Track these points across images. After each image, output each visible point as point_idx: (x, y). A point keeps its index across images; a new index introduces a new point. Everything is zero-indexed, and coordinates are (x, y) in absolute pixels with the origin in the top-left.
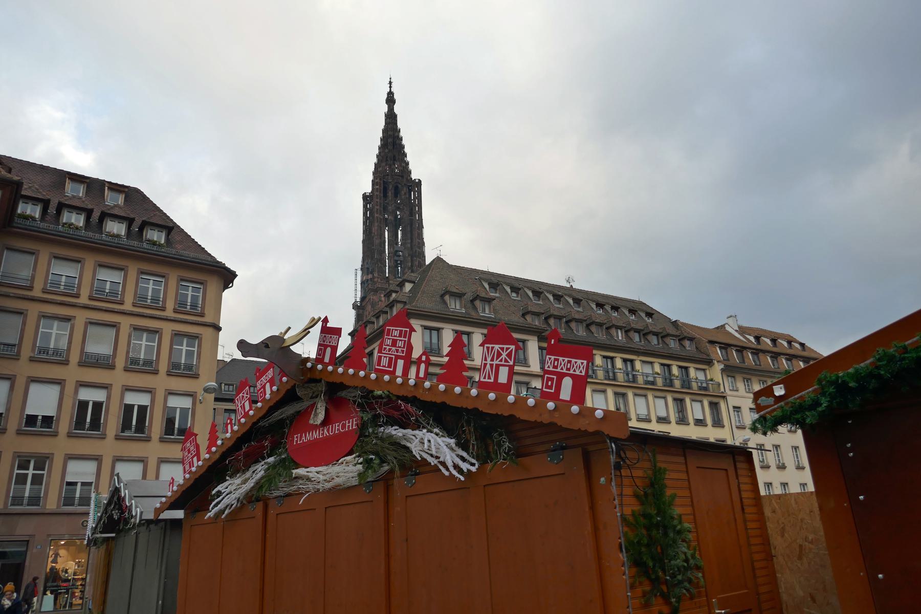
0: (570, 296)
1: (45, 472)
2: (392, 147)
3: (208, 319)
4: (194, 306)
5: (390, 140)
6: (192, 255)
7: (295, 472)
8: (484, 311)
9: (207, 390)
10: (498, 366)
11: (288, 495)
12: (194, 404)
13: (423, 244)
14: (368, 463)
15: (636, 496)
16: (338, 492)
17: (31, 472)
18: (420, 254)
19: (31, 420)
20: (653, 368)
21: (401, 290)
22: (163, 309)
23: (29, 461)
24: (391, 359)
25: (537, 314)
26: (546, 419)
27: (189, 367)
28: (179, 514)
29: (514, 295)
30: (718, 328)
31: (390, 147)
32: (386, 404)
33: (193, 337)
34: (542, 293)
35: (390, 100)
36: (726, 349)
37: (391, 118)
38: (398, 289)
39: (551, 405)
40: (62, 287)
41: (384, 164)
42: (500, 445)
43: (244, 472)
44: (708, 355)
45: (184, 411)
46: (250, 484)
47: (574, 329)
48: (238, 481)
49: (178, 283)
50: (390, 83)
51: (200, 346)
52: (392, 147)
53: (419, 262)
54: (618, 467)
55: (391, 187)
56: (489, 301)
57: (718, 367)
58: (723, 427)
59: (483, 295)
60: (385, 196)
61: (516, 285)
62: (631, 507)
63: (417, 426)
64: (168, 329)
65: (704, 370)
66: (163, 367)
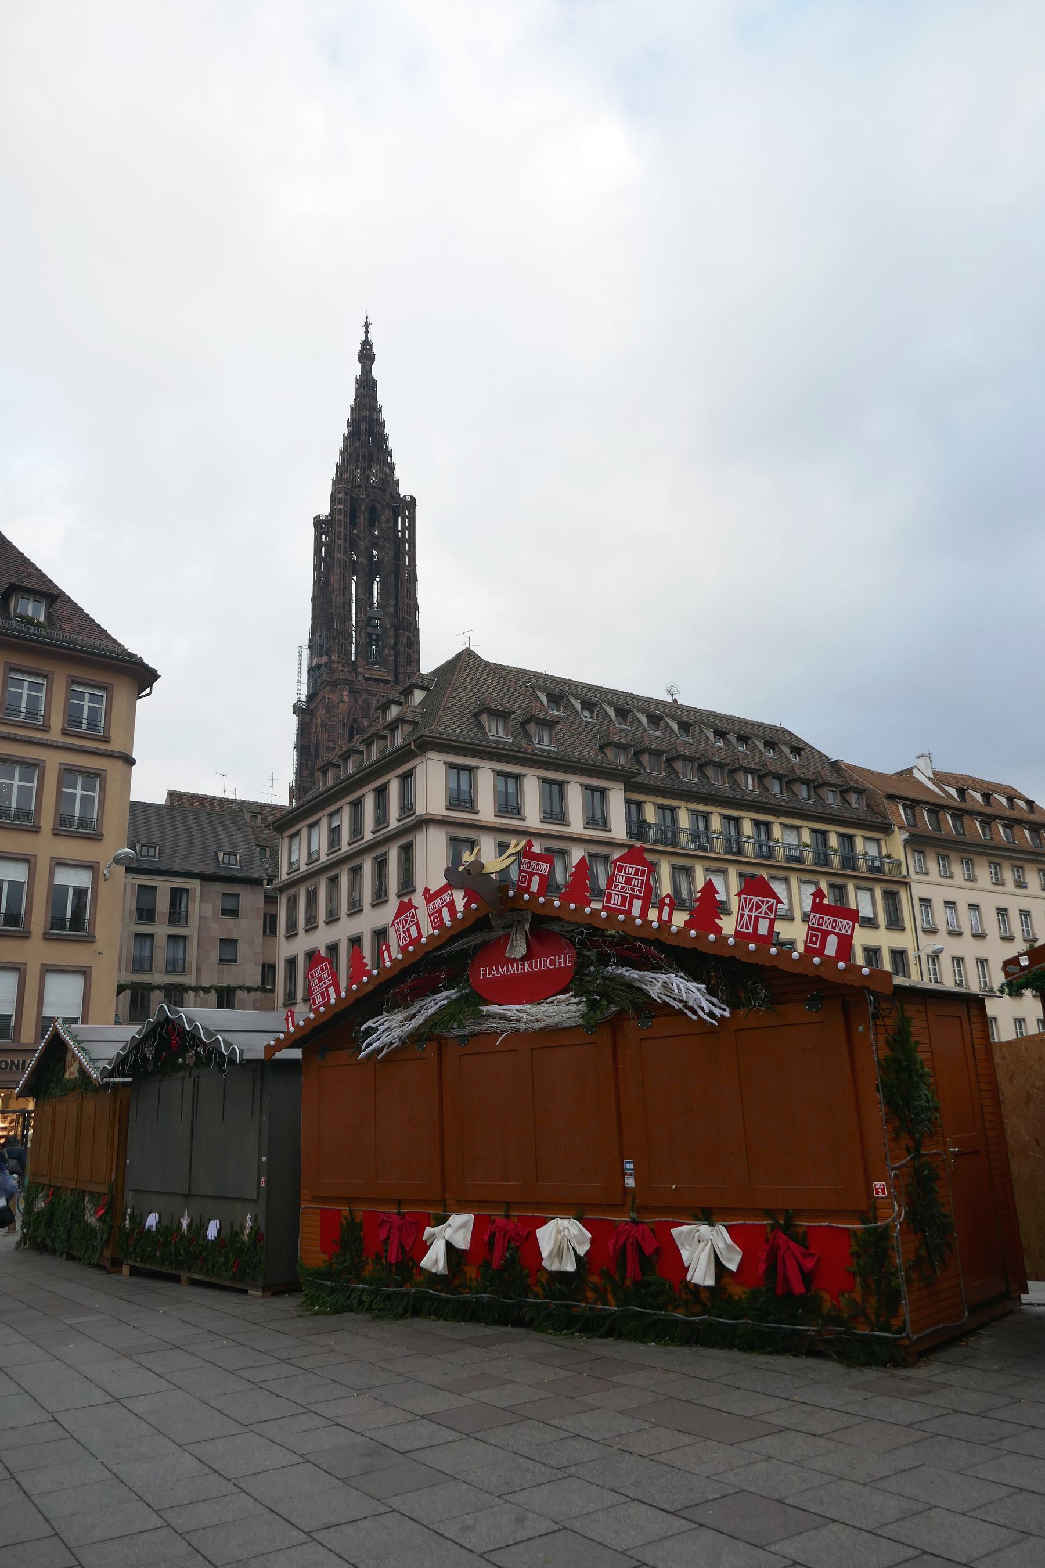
0: (673, 717)
2: (366, 437)
3: (115, 746)
4: (92, 725)
5: (364, 426)
6: (90, 641)
7: (485, 1009)
8: (541, 741)
9: (118, 860)
11: (476, 1034)
12: (95, 881)
13: (416, 607)
14: (592, 1005)
15: (887, 1042)
16: (550, 1035)
21: (407, 702)
22: (46, 728)
24: (624, 898)
25: (624, 747)
26: (810, 972)
27: (83, 822)
28: (296, 1054)
29: (586, 714)
30: (901, 773)
32: (617, 944)
33: (92, 776)
34: (630, 711)
35: (366, 355)
36: (912, 808)
37: (366, 386)
38: (401, 698)
39: (816, 960)
41: (352, 467)
42: (755, 992)
43: (406, 1007)
44: (885, 818)
45: (80, 893)
46: (419, 1020)
47: (680, 771)
48: (399, 1016)
49: (68, 686)
50: (367, 325)
51: (103, 789)
52: (366, 437)
53: (409, 638)
54: (875, 1017)
55: (363, 507)
56: (549, 724)
57: (899, 837)
58: (903, 929)
59: (541, 715)
61: (590, 697)
62: (885, 1052)
63: (655, 969)
64: (53, 761)
65: (877, 841)
66: (47, 821)
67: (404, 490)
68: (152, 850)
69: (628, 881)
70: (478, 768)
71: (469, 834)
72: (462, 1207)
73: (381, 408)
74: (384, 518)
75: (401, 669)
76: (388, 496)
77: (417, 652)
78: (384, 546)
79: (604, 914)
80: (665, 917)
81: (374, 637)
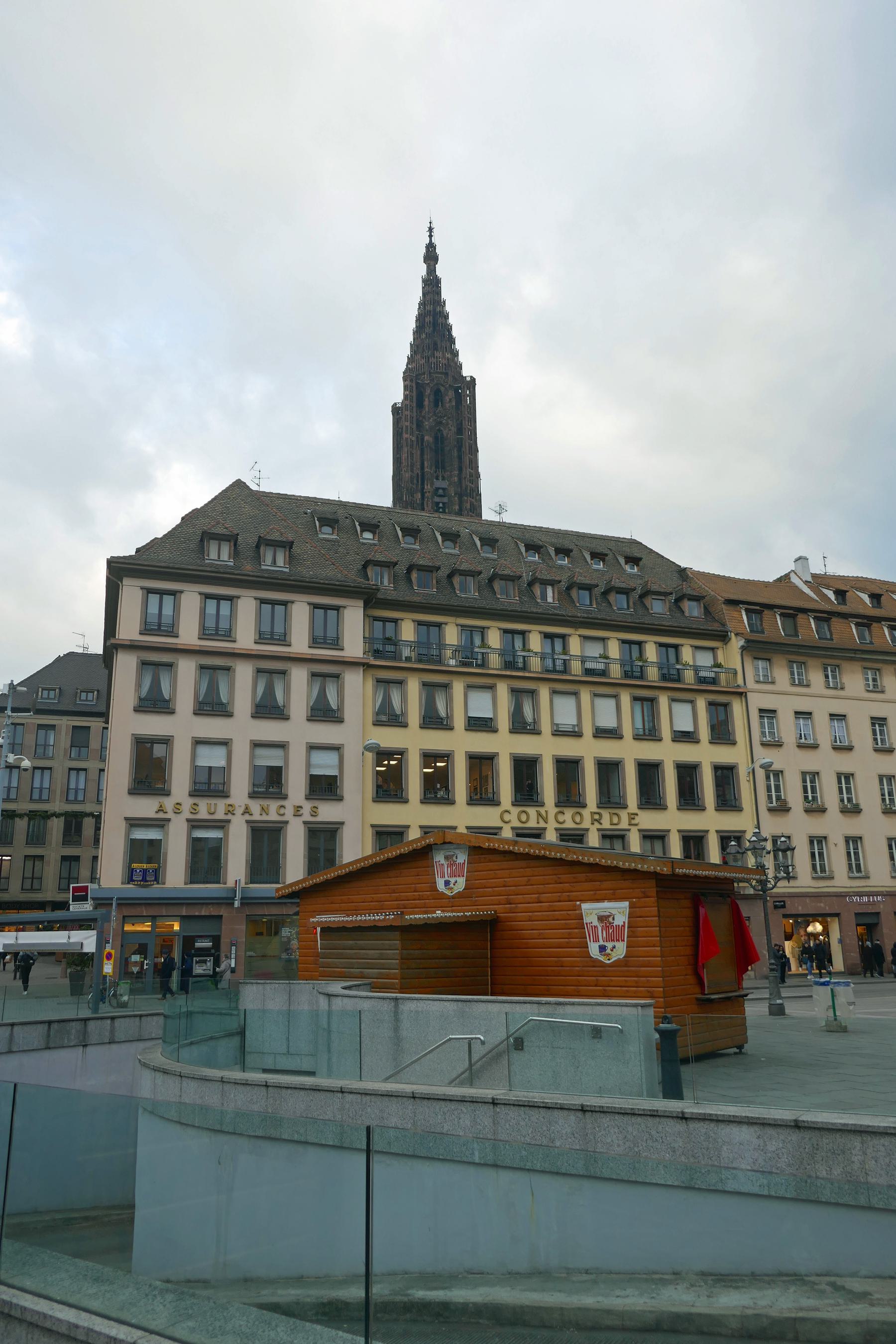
2: (433, 328)
5: (427, 320)
13: (478, 476)
18: (472, 490)
30: (780, 580)
31: (428, 330)
35: (431, 256)
37: (432, 284)
41: (419, 357)
44: (724, 625)
47: (457, 586)
50: (431, 230)
52: (433, 328)
53: (472, 504)
55: (428, 391)
57: (736, 643)
58: (734, 743)
60: (420, 405)
65: (713, 649)
68: (90, 695)
70: (181, 592)
71: (165, 658)
73: (444, 302)
74: (447, 399)
76: (450, 379)
78: (448, 424)
81: (441, 505)
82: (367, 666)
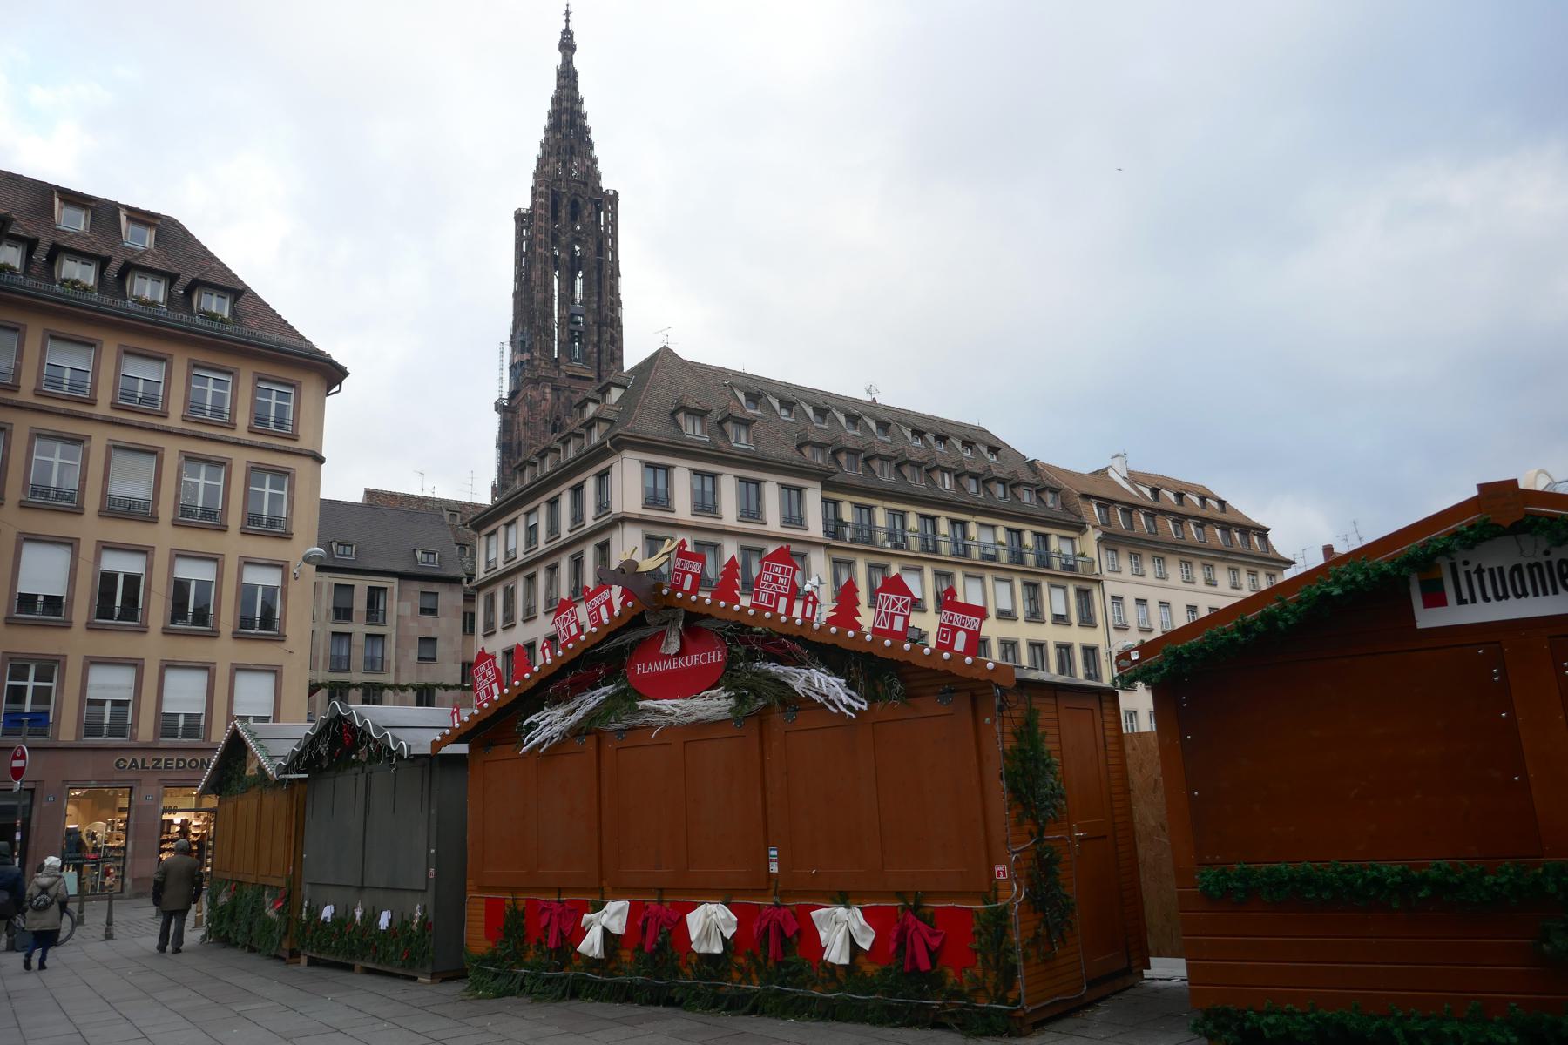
0: (871, 416)
1: (53, 684)
2: (567, 129)
3: (302, 445)
4: (280, 423)
5: (564, 118)
6: (275, 337)
7: (641, 704)
8: (739, 439)
9: (307, 559)
10: (893, 615)
11: (632, 728)
12: (285, 580)
13: (619, 304)
14: (741, 699)
15: (1014, 734)
16: (702, 728)
17: (30, 684)
18: (613, 320)
19: (27, 601)
20: (995, 535)
21: (604, 399)
22: (232, 426)
23: (27, 667)
24: (771, 596)
25: (821, 446)
26: (940, 667)
27: (272, 521)
28: (463, 748)
29: (785, 412)
30: (1096, 473)
32: (764, 640)
33: (280, 474)
34: (828, 411)
35: (567, 45)
36: (1106, 507)
37: (567, 77)
38: (598, 396)
39: (946, 655)
40: (66, 387)
42: (891, 686)
43: (567, 702)
44: (1080, 517)
45: (270, 592)
46: (580, 714)
48: (560, 711)
49: (254, 384)
50: (567, 13)
51: (292, 488)
52: (567, 129)
53: (612, 336)
54: (1001, 709)
55: (565, 201)
56: (746, 423)
57: (1093, 535)
59: (738, 414)
60: (555, 217)
61: (789, 396)
62: (1010, 743)
63: (800, 664)
64: (240, 459)
65: (1072, 539)
66: (235, 520)
67: (606, 184)
69: (775, 579)
72: (618, 894)
74: (586, 213)
75: (604, 367)
76: (590, 190)
77: (621, 349)
79: (751, 611)
80: (808, 614)
82: (828, 547)
